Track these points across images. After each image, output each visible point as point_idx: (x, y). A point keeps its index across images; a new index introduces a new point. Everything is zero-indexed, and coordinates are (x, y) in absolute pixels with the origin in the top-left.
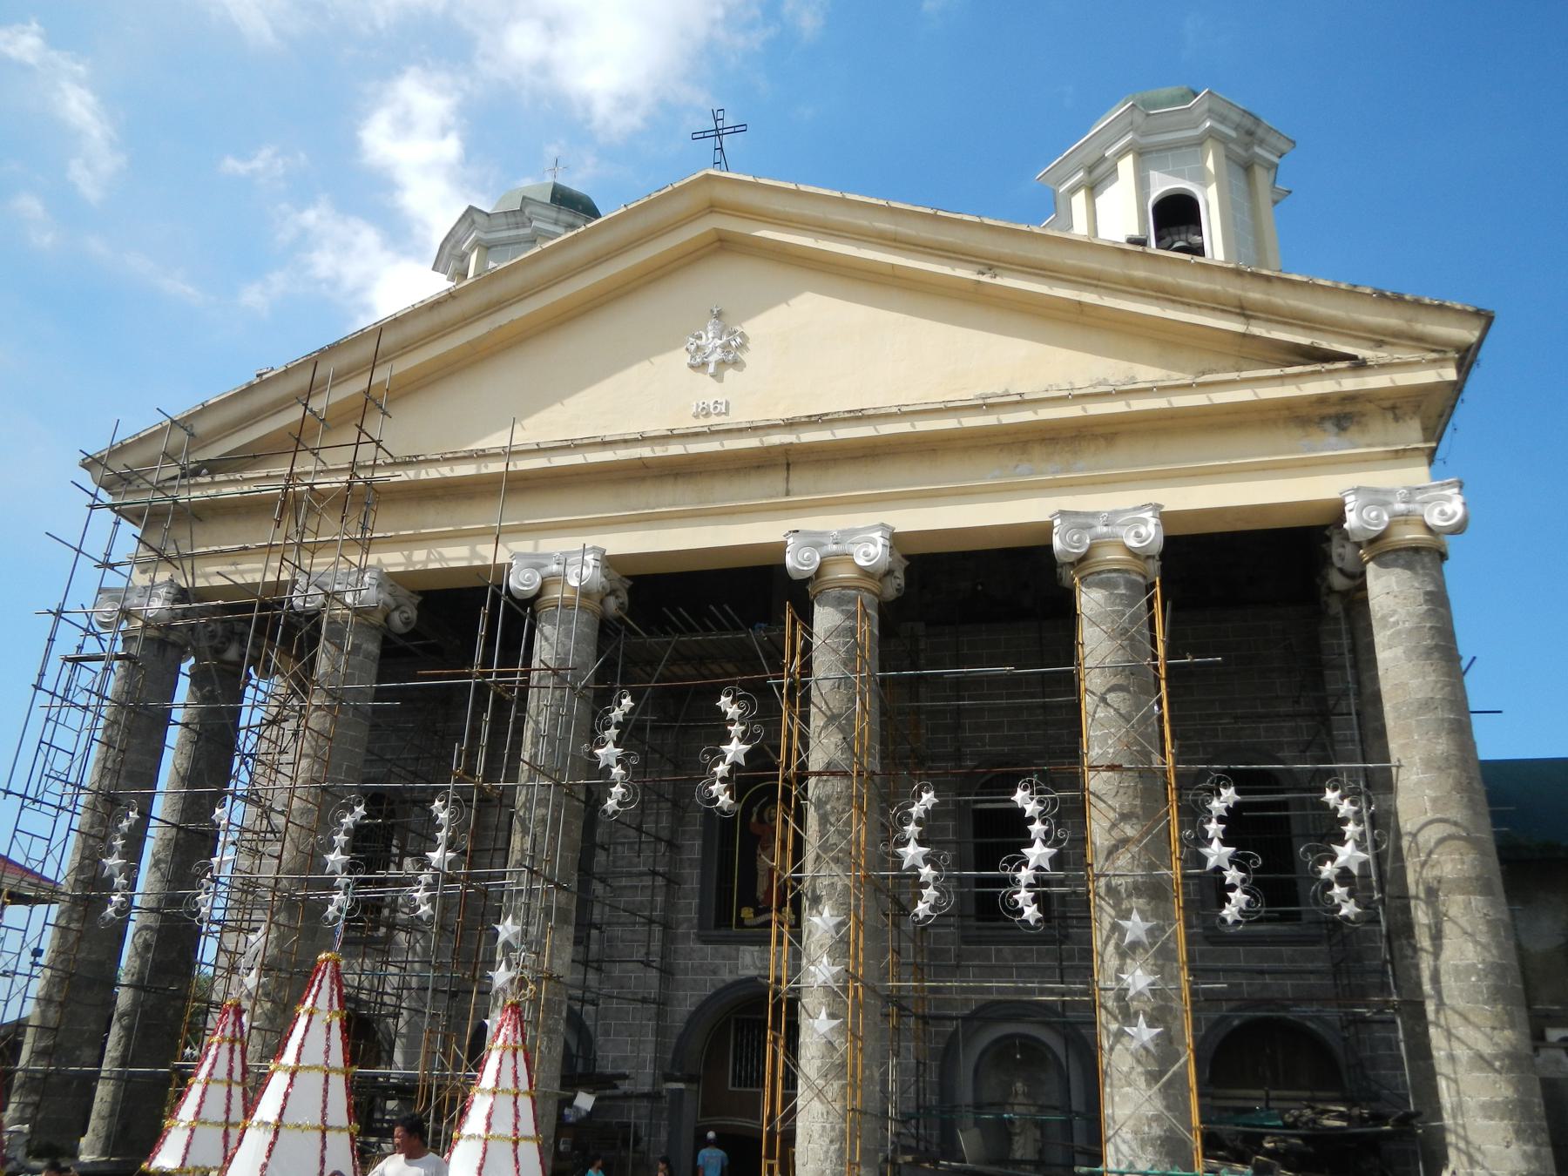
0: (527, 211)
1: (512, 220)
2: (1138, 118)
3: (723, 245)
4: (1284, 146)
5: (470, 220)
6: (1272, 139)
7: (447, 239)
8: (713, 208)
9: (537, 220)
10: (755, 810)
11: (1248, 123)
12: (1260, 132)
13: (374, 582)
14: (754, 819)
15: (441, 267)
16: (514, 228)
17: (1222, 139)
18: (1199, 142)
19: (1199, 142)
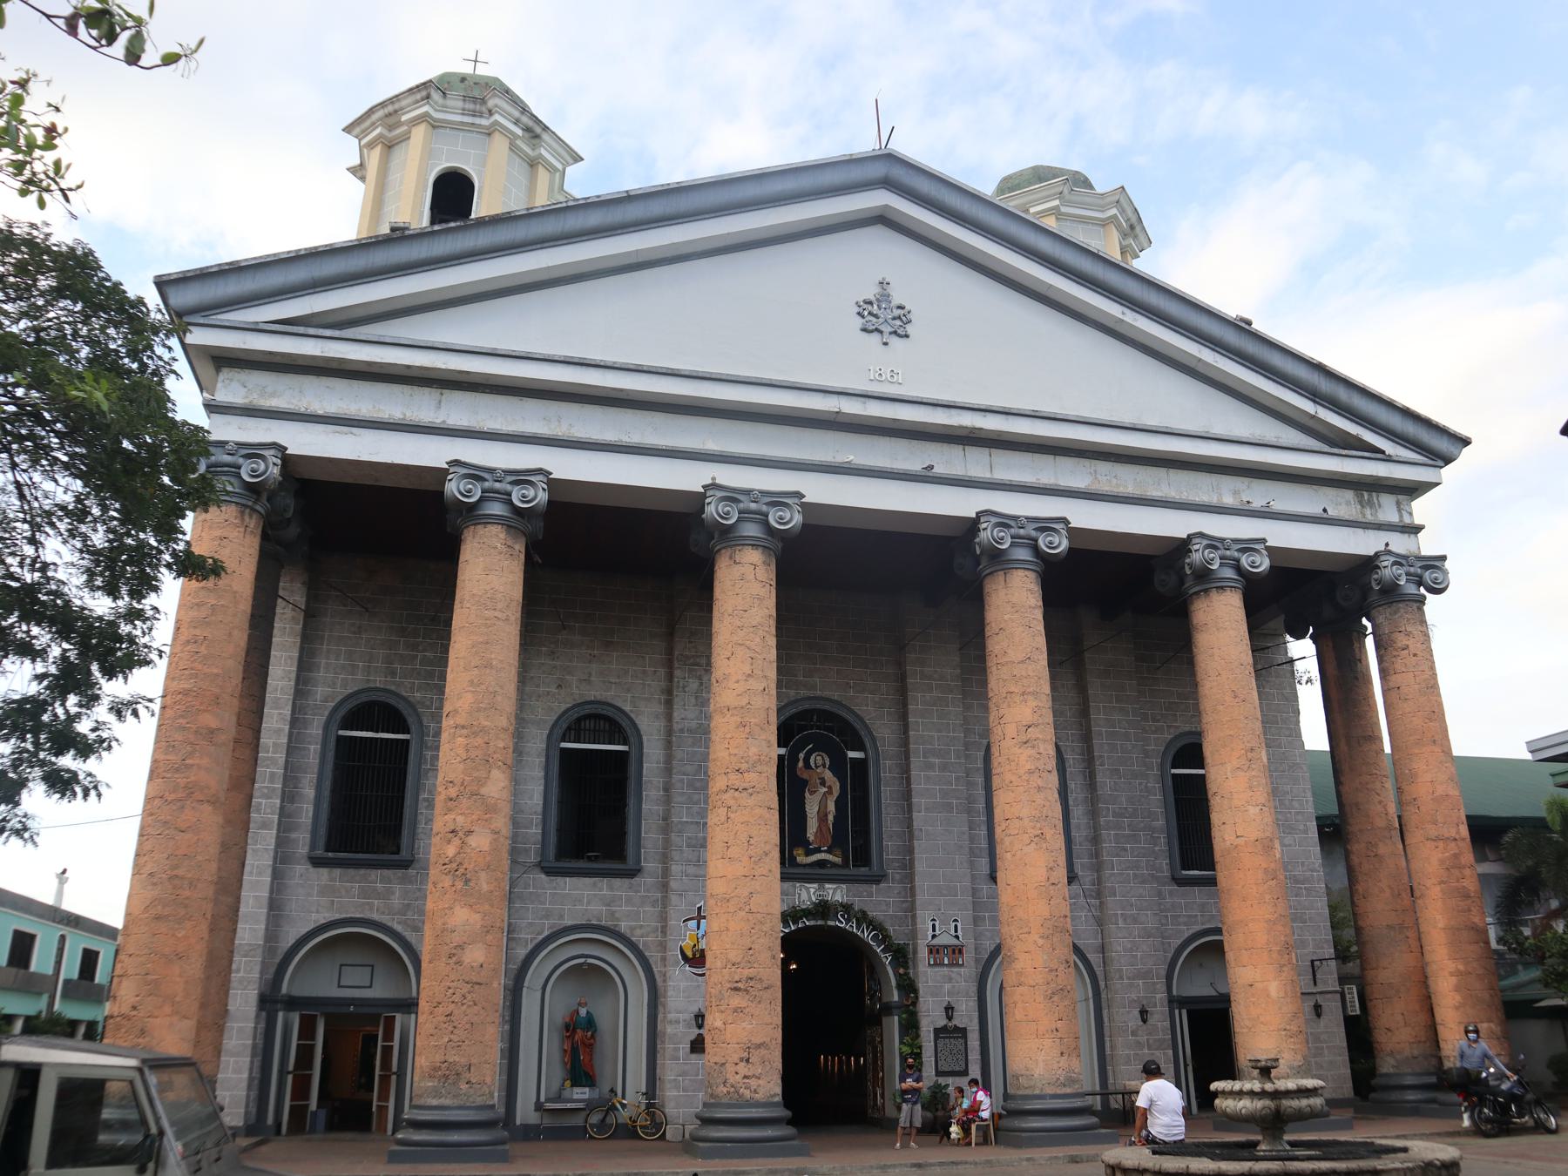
0: (491, 103)
1: (470, 106)
2: (1066, 191)
3: (883, 219)
4: (1146, 245)
5: (424, 93)
6: (1142, 237)
7: (382, 105)
8: (888, 184)
9: (500, 114)
10: (802, 756)
11: (1134, 219)
12: (1138, 229)
13: (546, 487)
14: (801, 764)
15: (357, 130)
16: (468, 115)
17: (1119, 227)
18: (1104, 223)
19: (1104, 223)
